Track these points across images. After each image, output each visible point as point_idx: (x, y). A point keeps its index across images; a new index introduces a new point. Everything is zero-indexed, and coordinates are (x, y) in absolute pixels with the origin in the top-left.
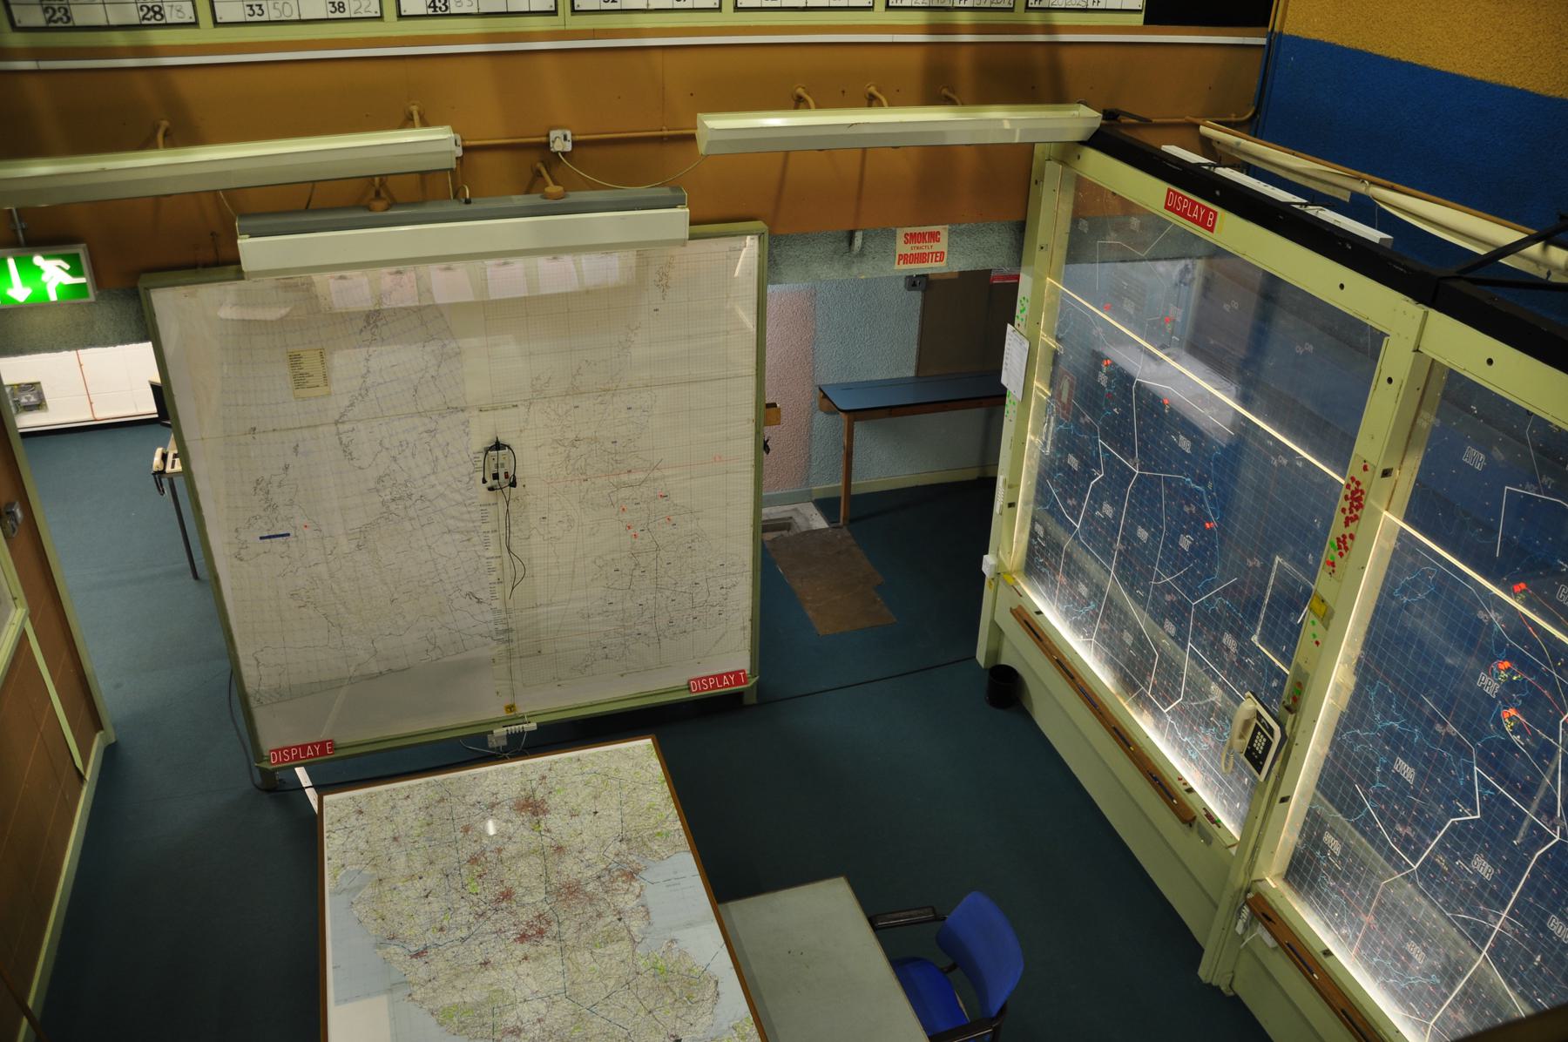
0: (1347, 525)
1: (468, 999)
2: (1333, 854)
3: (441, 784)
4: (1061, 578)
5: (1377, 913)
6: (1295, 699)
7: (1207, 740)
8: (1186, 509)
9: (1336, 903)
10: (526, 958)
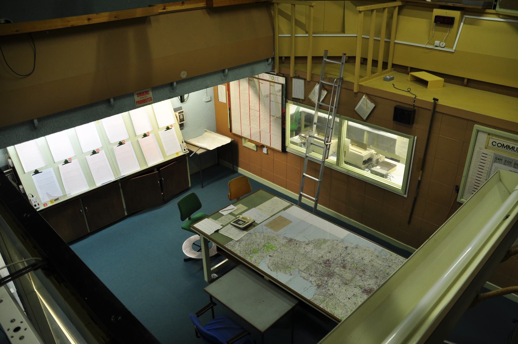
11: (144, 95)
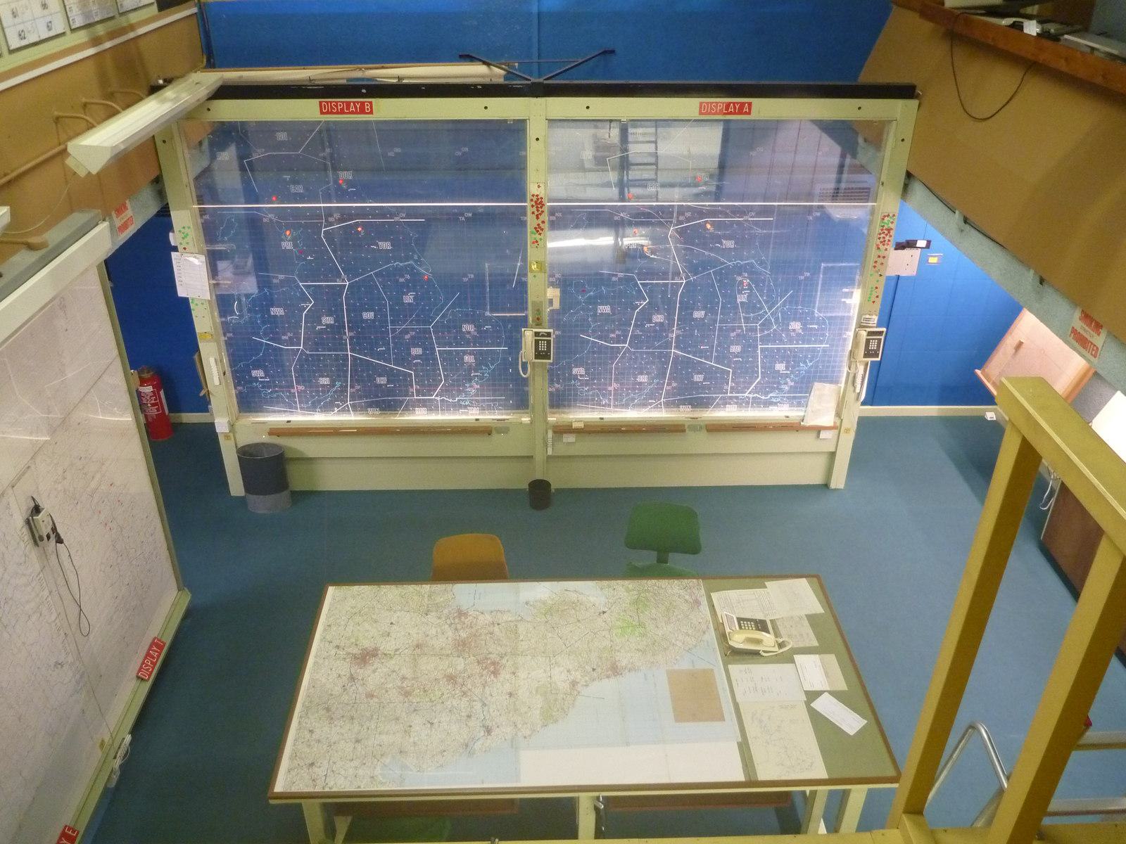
0: (538, 218)
1: (539, 706)
2: (581, 376)
3: (307, 709)
4: (298, 388)
5: (617, 380)
6: (538, 319)
7: (473, 388)
8: (402, 280)
9: (593, 395)
10: (514, 673)
11: (1089, 325)
